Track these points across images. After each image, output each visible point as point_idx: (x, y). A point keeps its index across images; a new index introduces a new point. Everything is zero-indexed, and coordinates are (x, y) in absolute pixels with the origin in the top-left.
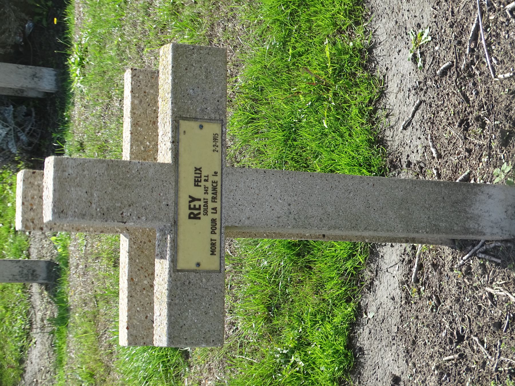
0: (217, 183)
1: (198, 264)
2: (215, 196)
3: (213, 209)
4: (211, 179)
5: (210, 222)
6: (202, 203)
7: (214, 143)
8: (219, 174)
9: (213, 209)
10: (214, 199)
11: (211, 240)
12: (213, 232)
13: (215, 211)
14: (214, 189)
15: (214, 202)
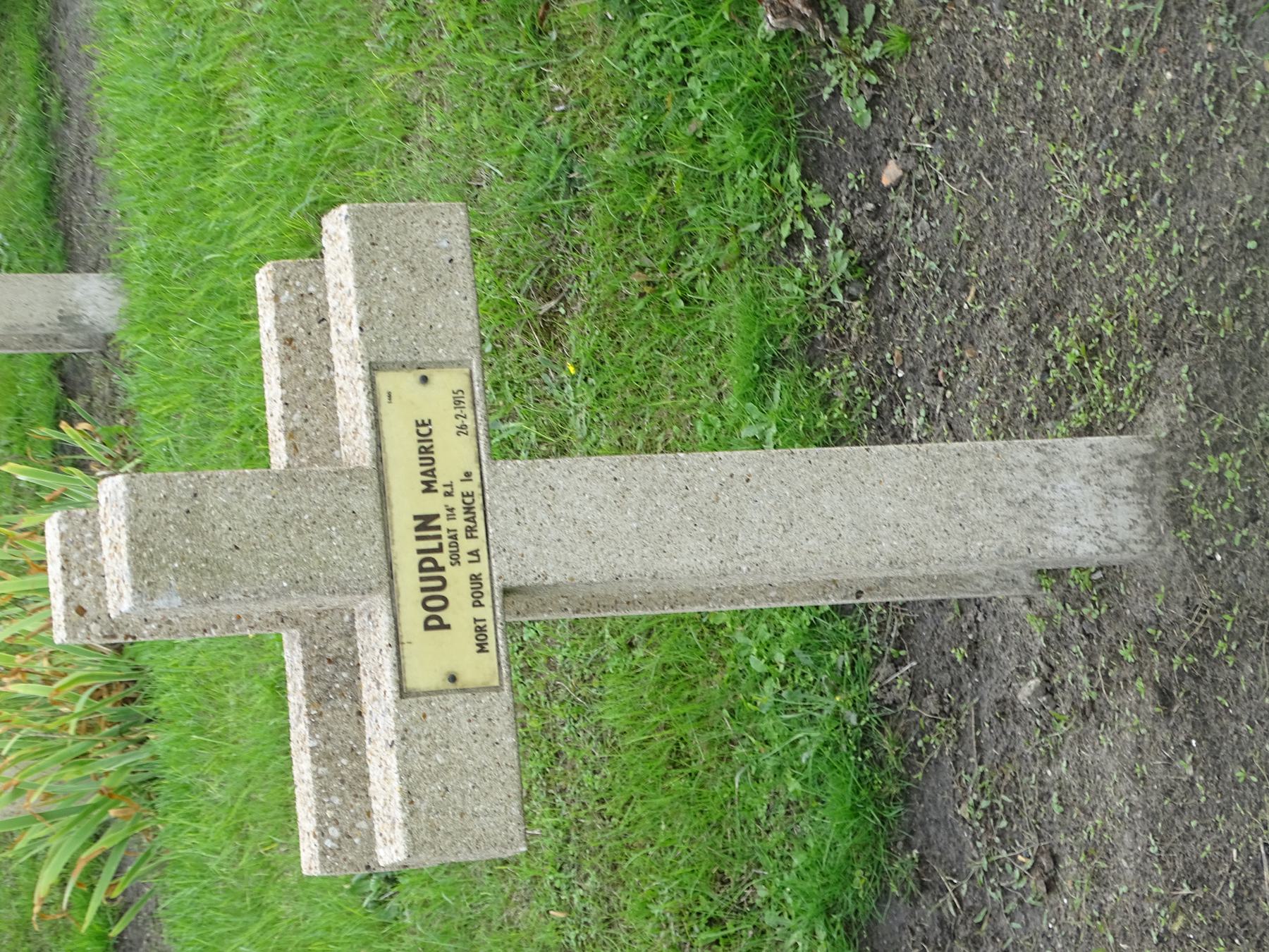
0: (472, 495)
1: (453, 679)
2: (472, 524)
3: (471, 553)
4: (459, 488)
5: (468, 581)
6: (446, 541)
7: (458, 411)
8: (476, 477)
9: (471, 553)
10: (470, 532)
11: (475, 620)
12: (477, 604)
13: (475, 558)
14: (469, 509)
15: (472, 537)
